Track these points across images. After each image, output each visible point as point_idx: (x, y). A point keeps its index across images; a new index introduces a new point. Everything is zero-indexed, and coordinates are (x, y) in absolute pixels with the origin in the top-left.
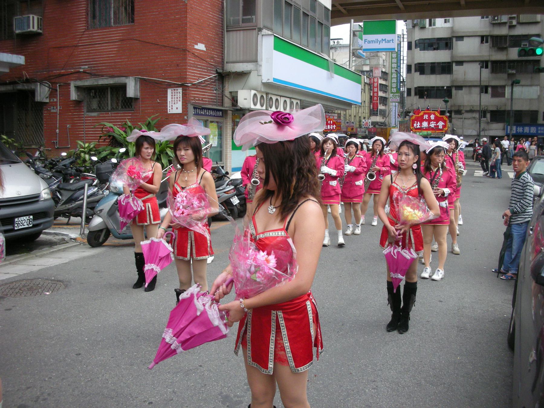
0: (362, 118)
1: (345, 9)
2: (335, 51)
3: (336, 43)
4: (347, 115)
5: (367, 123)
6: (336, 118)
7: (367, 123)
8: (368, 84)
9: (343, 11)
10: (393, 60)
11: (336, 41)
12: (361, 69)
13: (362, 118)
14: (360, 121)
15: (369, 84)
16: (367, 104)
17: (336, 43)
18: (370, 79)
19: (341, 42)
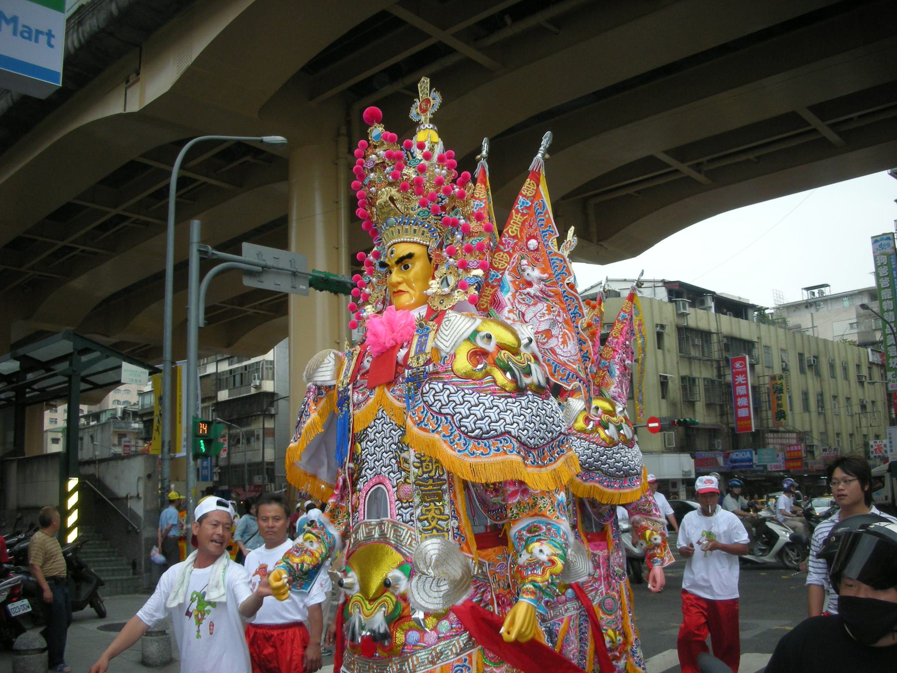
0: (871, 436)
1: (698, 167)
2: (817, 310)
3: (817, 295)
4: (831, 434)
5: (879, 448)
6: (794, 442)
7: (879, 448)
8: (877, 365)
9: (695, 175)
10: (883, 293)
11: (816, 291)
12: (870, 339)
13: (871, 436)
14: (866, 445)
15: (883, 366)
16: (881, 406)
17: (817, 295)
18: (882, 355)
19: (827, 292)
